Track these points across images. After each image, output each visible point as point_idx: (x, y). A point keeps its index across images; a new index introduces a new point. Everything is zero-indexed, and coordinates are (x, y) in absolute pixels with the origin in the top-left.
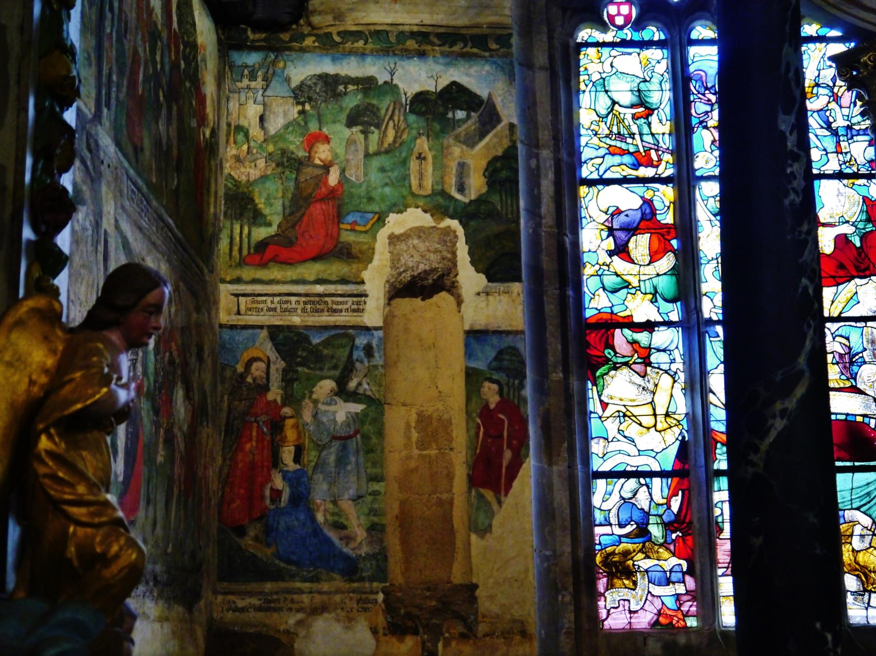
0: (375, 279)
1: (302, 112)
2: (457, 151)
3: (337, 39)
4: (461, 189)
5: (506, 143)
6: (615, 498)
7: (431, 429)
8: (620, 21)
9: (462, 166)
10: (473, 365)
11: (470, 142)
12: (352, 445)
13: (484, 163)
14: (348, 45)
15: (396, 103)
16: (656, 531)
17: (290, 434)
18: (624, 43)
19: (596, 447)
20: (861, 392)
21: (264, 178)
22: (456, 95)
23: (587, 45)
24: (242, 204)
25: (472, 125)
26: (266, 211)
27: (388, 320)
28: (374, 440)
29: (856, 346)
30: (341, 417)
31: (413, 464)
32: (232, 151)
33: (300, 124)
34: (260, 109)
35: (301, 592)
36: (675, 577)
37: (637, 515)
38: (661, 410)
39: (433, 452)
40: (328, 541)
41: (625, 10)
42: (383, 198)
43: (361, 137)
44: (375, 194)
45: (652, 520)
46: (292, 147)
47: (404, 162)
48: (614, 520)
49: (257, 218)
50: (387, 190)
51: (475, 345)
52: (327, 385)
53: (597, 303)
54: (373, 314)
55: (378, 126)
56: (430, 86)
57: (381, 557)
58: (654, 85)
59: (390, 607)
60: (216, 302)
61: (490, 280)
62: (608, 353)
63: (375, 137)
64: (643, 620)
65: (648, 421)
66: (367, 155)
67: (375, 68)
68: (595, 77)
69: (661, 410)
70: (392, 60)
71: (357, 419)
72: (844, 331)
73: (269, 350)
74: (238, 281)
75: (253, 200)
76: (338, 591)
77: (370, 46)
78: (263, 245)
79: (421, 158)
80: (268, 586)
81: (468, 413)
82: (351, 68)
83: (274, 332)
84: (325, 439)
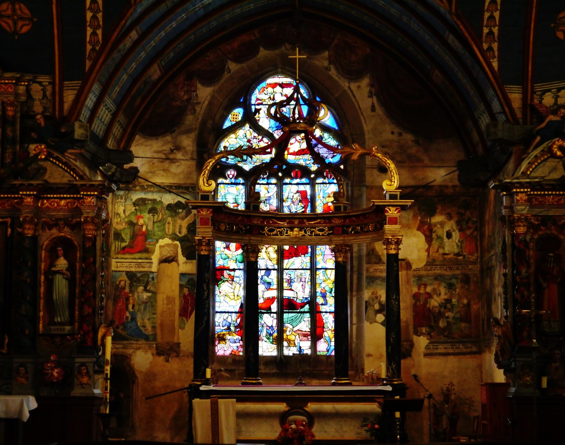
0: (155, 258)
1: (135, 209)
2: (179, 221)
3: (146, 187)
4: (180, 233)
5: (193, 219)
6: (221, 320)
7: (170, 300)
8: (231, 176)
9: (180, 226)
10: (181, 283)
11: (183, 219)
12: (148, 304)
13: (187, 225)
14: (149, 189)
15: (162, 207)
16: (232, 328)
17: (131, 301)
18: (232, 184)
19: (217, 304)
20: (293, 290)
21: (124, 229)
22: (178, 205)
23: (221, 184)
24: (118, 236)
25: (183, 214)
26: (125, 238)
27: (159, 270)
28: (154, 303)
29: (293, 277)
30: (145, 297)
31: (164, 309)
32: (116, 220)
33: (135, 213)
34: (123, 208)
35: (133, 344)
36: (237, 341)
37: (228, 324)
38: (236, 295)
39: (170, 306)
40: (141, 331)
41: (233, 173)
42: (158, 235)
43: (152, 217)
44: (156, 234)
45: (232, 325)
46: (133, 220)
47: (164, 225)
48: (221, 325)
49: (123, 240)
50: (159, 233)
51: (182, 278)
52: (141, 288)
53: (219, 262)
54: (154, 268)
55: (157, 214)
56: (172, 202)
57: (155, 335)
58: (240, 197)
59: (157, 348)
60: (111, 265)
61: (187, 259)
62: (222, 277)
63: (156, 217)
64: (228, 353)
65: (232, 297)
66: (154, 222)
67: (156, 196)
68: (223, 194)
69: (236, 295)
70: (161, 194)
71: (149, 297)
72: (289, 273)
73: (125, 278)
74: (117, 258)
75: (121, 235)
76: (143, 344)
77: (155, 190)
78: (124, 248)
79: (169, 223)
80: (125, 342)
81: (180, 297)
82: (149, 196)
83: (127, 273)
84: (141, 303)
